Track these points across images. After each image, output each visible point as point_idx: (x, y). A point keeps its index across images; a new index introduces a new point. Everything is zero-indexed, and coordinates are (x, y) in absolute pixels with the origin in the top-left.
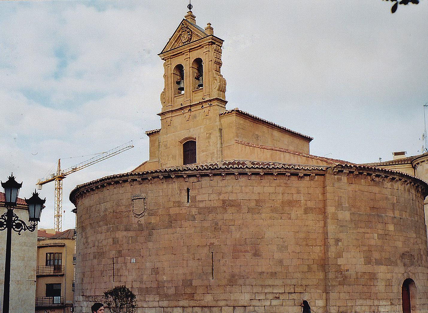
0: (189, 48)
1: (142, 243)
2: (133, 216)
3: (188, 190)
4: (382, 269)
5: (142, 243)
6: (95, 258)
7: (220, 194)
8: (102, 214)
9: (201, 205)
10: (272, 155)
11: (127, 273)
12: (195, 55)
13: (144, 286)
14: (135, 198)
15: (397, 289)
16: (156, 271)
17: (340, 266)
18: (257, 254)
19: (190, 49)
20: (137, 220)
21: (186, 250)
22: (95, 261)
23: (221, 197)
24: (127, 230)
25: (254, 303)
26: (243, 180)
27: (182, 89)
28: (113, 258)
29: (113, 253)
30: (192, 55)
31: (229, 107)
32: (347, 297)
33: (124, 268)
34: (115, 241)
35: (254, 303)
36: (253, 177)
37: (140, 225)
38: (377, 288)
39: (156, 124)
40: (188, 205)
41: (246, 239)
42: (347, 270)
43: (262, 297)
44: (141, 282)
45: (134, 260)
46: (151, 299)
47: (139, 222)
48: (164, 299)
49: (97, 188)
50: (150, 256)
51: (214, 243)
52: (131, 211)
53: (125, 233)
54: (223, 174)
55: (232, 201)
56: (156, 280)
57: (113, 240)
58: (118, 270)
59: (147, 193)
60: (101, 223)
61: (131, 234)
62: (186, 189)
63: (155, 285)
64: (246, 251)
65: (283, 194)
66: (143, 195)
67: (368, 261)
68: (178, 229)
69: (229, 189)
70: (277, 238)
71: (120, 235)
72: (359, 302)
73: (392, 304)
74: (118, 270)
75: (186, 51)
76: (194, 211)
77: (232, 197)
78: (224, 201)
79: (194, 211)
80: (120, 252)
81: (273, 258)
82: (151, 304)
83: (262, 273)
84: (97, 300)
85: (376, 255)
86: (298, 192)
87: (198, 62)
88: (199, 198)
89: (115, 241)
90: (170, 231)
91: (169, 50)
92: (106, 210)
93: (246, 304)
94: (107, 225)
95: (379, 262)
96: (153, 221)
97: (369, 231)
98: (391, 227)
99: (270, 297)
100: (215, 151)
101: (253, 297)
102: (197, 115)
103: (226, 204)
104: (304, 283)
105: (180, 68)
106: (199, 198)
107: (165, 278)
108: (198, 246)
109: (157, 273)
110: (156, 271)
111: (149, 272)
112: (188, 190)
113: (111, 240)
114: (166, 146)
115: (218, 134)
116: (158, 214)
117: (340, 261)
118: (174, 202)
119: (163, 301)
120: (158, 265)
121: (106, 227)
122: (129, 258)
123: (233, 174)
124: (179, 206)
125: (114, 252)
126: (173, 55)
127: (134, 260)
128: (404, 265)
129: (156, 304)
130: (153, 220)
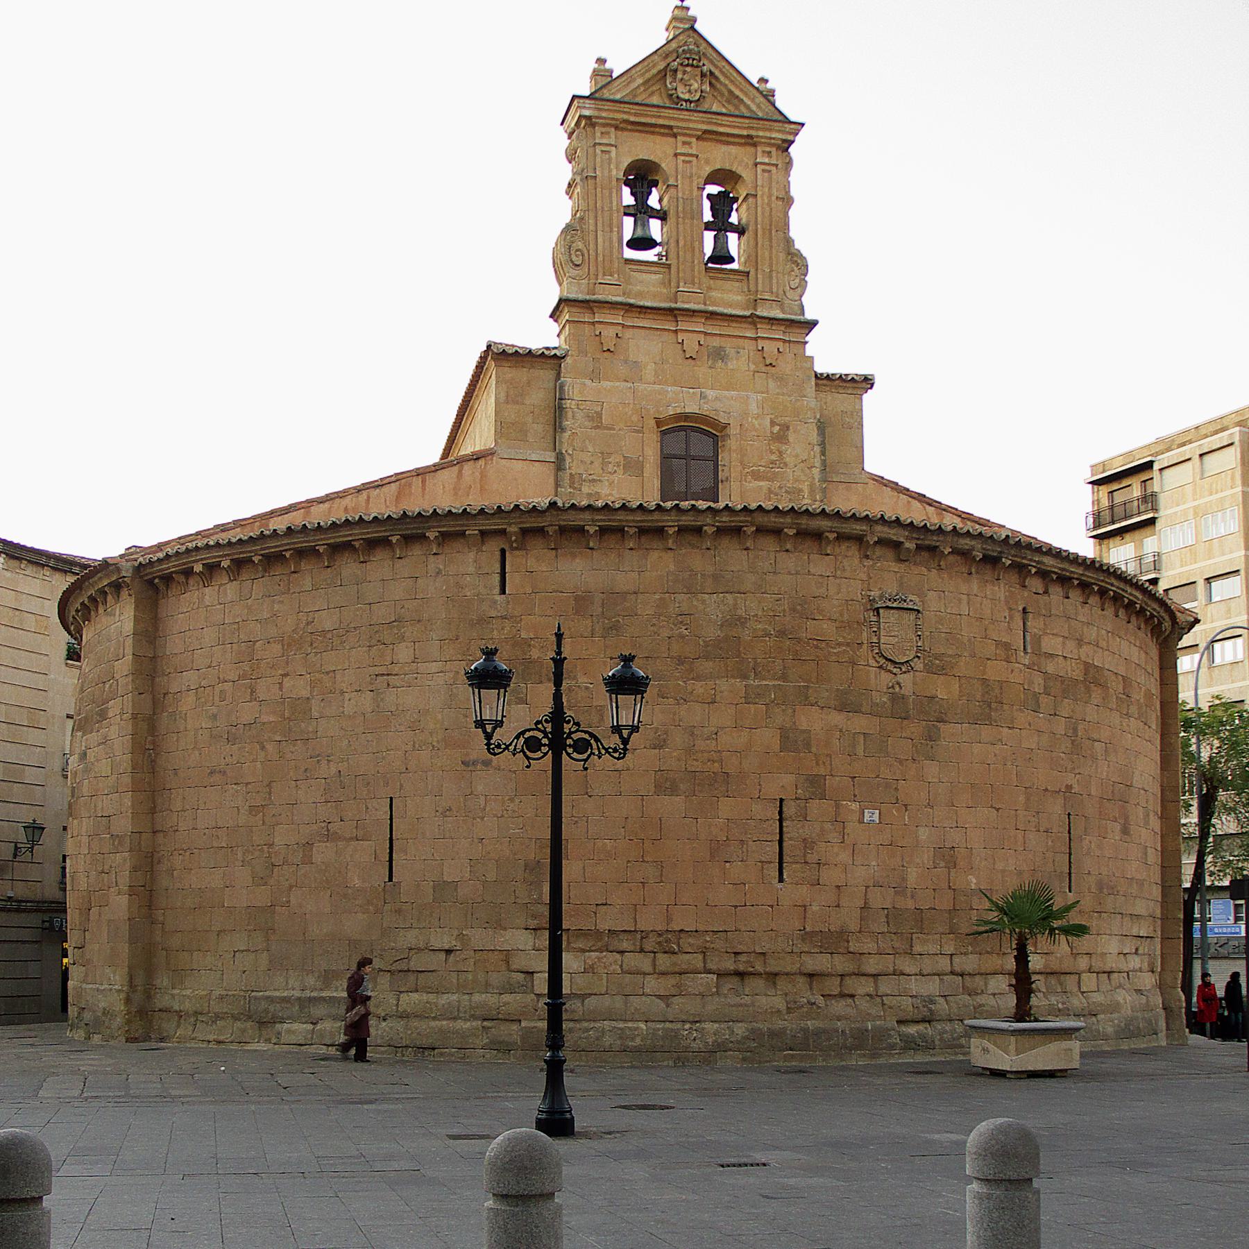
0: (705, 127)
2: (872, 662)
7: (1080, 642)
9: (1050, 668)
11: (844, 857)
13: (910, 904)
16: (947, 856)
19: (705, 132)
20: (886, 678)
21: (1022, 799)
24: (846, 705)
30: (681, 147)
33: (834, 837)
34: (791, 741)
37: (897, 698)
44: (900, 890)
46: (933, 948)
52: (865, 646)
53: (837, 718)
58: (808, 844)
59: (921, 595)
61: (859, 723)
63: (945, 903)
71: (813, 721)
74: (808, 844)
75: (688, 129)
76: (1038, 683)
82: (928, 965)
84: (679, 946)
89: (791, 741)
90: (986, 732)
91: (618, 97)
94: (745, 677)
96: (941, 694)
100: (805, 488)
102: (731, 352)
108: (1046, 790)
109: (952, 864)
110: (947, 856)
111: (926, 857)
113: (768, 737)
114: (596, 420)
115: (814, 437)
116: (955, 672)
118: (998, 643)
120: (955, 838)
121: (739, 683)
122: (855, 806)
126: (633, 123)
127: (871, 816)
130: (944, 689)
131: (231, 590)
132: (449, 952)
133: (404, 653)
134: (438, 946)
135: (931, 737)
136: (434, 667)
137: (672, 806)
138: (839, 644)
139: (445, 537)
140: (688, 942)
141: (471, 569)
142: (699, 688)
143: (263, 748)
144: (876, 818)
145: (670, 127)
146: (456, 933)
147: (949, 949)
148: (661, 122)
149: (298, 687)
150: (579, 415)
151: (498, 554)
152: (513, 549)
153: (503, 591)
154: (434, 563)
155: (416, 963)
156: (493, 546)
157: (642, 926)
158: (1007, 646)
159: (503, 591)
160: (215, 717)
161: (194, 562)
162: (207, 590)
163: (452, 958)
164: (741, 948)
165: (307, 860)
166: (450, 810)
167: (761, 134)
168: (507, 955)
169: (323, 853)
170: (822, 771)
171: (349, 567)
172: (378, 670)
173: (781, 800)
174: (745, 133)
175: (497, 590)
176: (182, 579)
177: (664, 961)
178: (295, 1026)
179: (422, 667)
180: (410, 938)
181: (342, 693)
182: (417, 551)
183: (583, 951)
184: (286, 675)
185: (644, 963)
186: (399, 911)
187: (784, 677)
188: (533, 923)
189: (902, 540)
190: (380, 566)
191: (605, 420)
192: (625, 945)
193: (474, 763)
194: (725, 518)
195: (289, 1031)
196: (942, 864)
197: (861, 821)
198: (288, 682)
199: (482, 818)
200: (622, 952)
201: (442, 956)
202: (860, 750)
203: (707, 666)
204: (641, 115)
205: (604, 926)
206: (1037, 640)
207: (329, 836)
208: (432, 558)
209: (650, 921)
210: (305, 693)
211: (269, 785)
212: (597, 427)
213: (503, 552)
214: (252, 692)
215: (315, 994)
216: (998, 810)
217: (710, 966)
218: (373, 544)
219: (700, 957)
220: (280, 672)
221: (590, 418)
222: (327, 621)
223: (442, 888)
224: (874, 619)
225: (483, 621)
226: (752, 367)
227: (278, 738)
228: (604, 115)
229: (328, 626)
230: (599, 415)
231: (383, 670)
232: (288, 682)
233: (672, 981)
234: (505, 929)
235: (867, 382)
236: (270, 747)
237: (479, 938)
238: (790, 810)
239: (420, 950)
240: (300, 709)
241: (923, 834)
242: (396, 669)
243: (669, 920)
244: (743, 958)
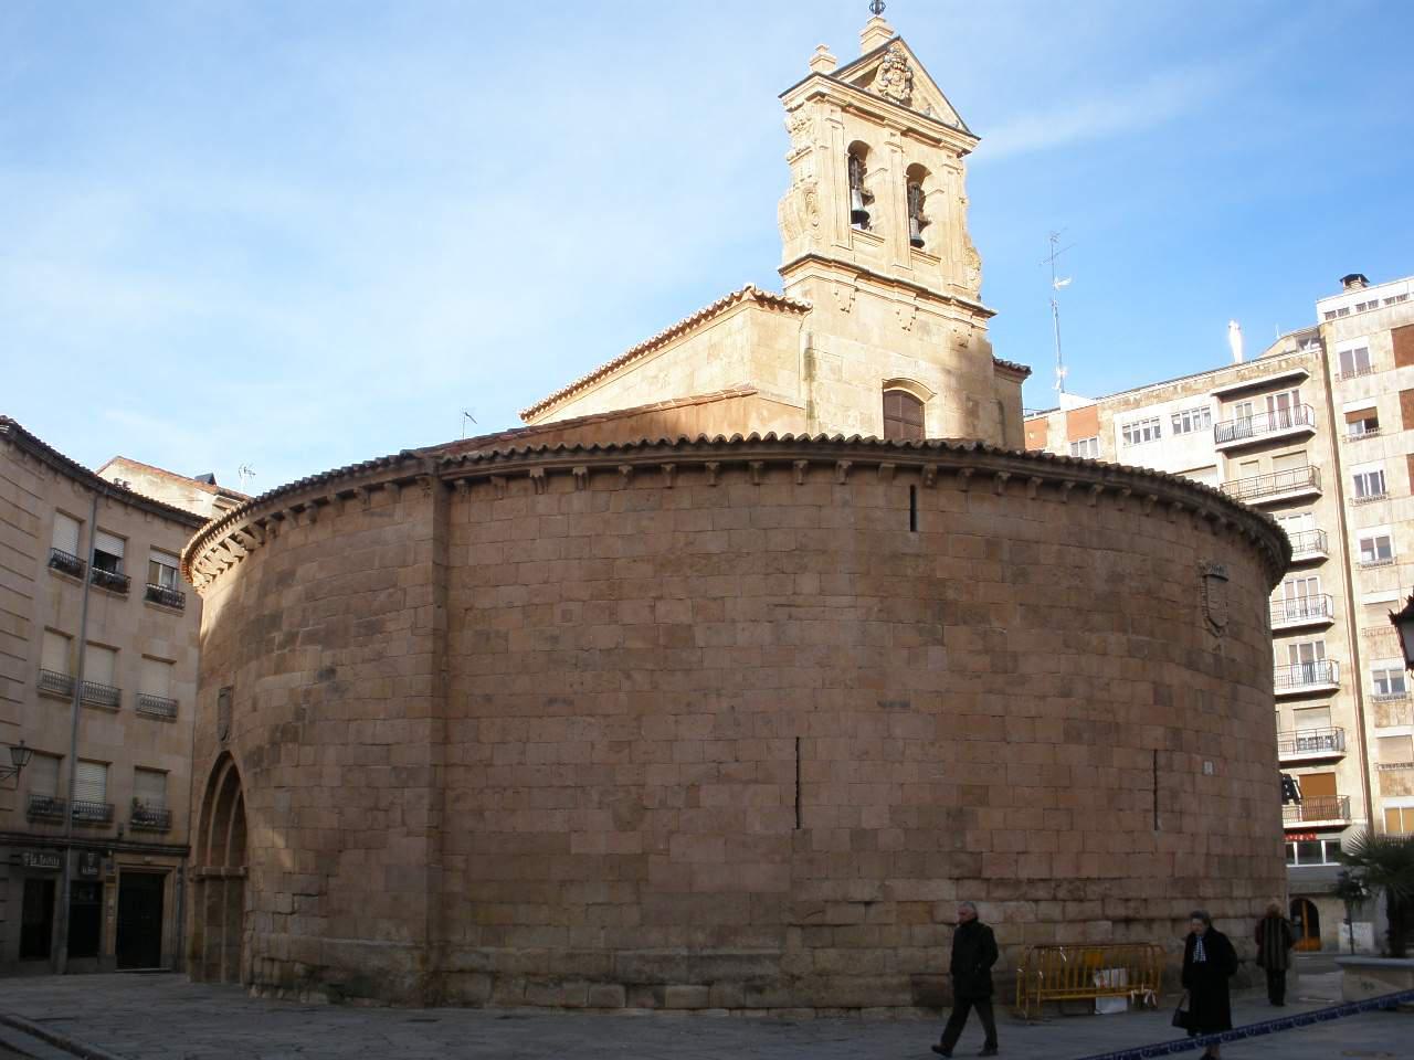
2: (1203, 625)
24: (1191, 665)
28: (1156, 751)
29: (1155, 735)
34: (1161, 696)
45: (1209, 768)
52: (1199, 609)
57: (1156, 692)
58: (1174, 795)
75: (896, 122)
80: (1176, 733)
89: (1161, 696)
94: (1125, 631)
102: (934, 329)
113: (1144, 690)
121: (1124, 639)
122: (1199, 758)
126: (857, 108)
131: (579, 500)
132: (868, 904)
133: (808, 584)
134: (858, 897)
136: (845, 601)
137: (1077, 754)
139: (856, 468)
140: (1094, 890)
141: (881, 502)
142: (1094, 639)
143: (629, 677)
145: (883, 118)
146: (877, 883)
148: (877, 112)
149: (683, 616)
151: (908, 491)
152: (926, 487)
153: (913, 528)
154: (840, 494)
155: (831, 916)
156: (905, 481)
157: (1058, 874)
159: (913, 528)
160: (555, 639)
161: (530, 465)
162: (541, 498)
163: (873, 909)
164: (1131, 894)
165: (694, 804)
166: (867, 753)
167: (948, 139)
168: (931, 907)
169: (712, 797)
171: (737, 487)
172: (776, 600)
175: (908, 527)
176: (501, 482)
177: (1073, 909)
178: (682, 988)
179: (831, 601)
180: (826, 890)
181: (733, 621)
182: (821, 478)
183: (1003, 900)
184: (660, 598)
185: (1054, 911)
186: (811, 861)
187: (1152, 634)
188: (956, 873)
189: (1219, 514)
190: (776, 490)
191: (845, 376)
192: (1041, 893)
193: (892, 704)
194: (1112, 478)
195: (676, 995)
198: (661, 607)
199: (901, 763)
200: (1036, 901)
201: (862, 909)
203: (1097, 618)
204: (867, 103)
205: (1024, 874)
207: (721, 778)
208: (838, 488)
209: (1062, 870)
210: (685, 619)
211: (638, 718)
212: (839, 380)
213: (913, 489)
214: (611, 614)
215: (706, 952)
217: (1110, 912)
218: (769, 467)
219: (1099, 903)
220: (653, 594)
221: (833, 370)
222: (714, 545)
223: (860, 836)
224: (1203, 585)
225: (896, 556)
227: (650, 666)
228: (836, 94)
229: (713, 548)
230: (840, 370)
231: (783, 600)
232: (661, 607)
233: (1079, 928)
234: (929, 879)
235: (1028, 371)
236: (638, 676)
237: (902, 888)
238: (1162, 760)
239: (836, 902)
240: (679, 636)
242: (799, 600)
243: (1078, 868)
244: (1132, 904)
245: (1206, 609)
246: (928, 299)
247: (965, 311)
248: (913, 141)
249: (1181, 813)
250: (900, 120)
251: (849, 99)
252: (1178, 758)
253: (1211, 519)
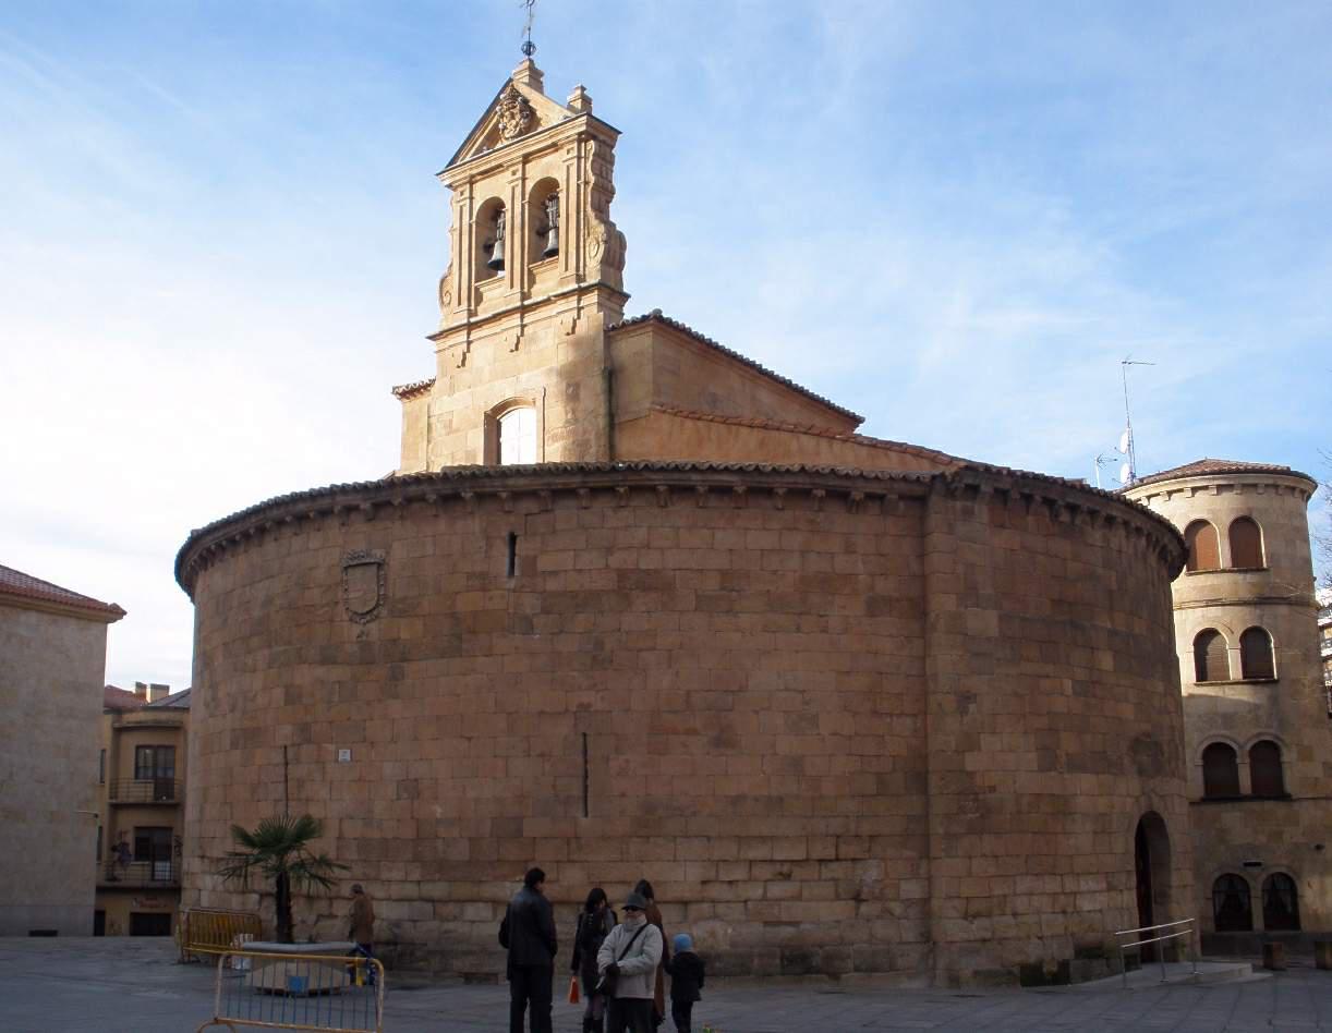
1: (368, 703)
3: (513, 539)
4: (1086, 782)
5: (368, 703)
6: (234, 745)
8: (257, 613)
9: (552, 585)
10: (762, 444)
12: (536, 172)
13: (376, 835)
14: (351, 563)
15: (1125, 844)
16: (411, 788)
17: (971, 774)
18: (723, 740)
20: (356, 629)
22: (237, 755)
23: (616, 560)
24: (327, 660)
25: (715, 891)
26: (682, 510)
27: (499, 265)
28: (285, 747)
29: (286, 731)
31: (631, 311)
32: (992, 871)
34: (292, 696)
35: (715, 891)
36: (713, 501)
37: (365, 646)
38: (1072, 842)
39: (422, 364)
40: (512, 584)
41: (688, 693)
42: (993, 789)
43: (739, 873)
45: (345, 755)
46: (396, 875)
47: (364, 638)
48: (437, 876)
49: (246, 536)
50: (395, 742)
51: (589, 705)
53: (320, 671)
54: (622, 490)
55: (647, 572)
56: (412, 818)
57: (287, 694)
58: (301, 783)
59: (388, 548)
60: (255, 642)
61: (338, 673)
62: (505, 534)
64: (693, 732)
65: (803, 553)
66: (378, 553)
67: (1049, 760)
68: (482, 659)
69: (641, 534)
70: (787, 689)
71: (305, 676)
72: (1024, 884)
73: (1111, 888)
76: (530, 604)
77: (649, 562)
78: (622, 574)
79: (530, 604)
80: (304, 729)
81: (775, 754)
82: (395, 890)
83: (737, 800)
85: (1068, 744)
86: (849, 550)
87: (547, 191)
88: (544, 563)
92: (269, 601)
93: (687, 895)
94: (270, 646)
95: (1076, 765)
96: (404, 635)
97: (1049, 669)
98: (1106, 661)
99: (764, 872)
101: (711, 874)
103: (630, 584)
104: (866, 828)
105: (494, 209)
106: (544, 563)
107: (438, 811)
110: (411, 788)
112: (513, 539)
113: (278, 693)
117: (972, 762)
118: (470, 576)
119: (433, 881)
122: (331, 747)
123: (653, 489)
124: (484, 589)
125: (287, 729)
127: (345, 755)
128: (1141, 772)
129: (410, 890)
130: (406, 631)
135: (396, 677)
138: (323, 606)
144: (348, 757)
145: (500, 166)
147: (416, 876)
148: (493, 164)
150: (439, 425)
158: (483, 575)
167: (560, 137)
170: (309, 719)
173: (285, 747)
174: (549, 142)
191: (454, 426)
196: (405, 795)
197: (337, 761)
202: (336, 698)
206: (531, 562)
212: (448, 434)
216: (469, 739)
226: (557, 341)
228: (457, 178)
241: (389, 769)
245: (346, 601)
246: (535, 309)
247: (570, 299)
248: (538, 161)
249: (307, 800)
250: (513, 156)
251: (468, 173)
252: (306, 749)
253: (350, 509)
